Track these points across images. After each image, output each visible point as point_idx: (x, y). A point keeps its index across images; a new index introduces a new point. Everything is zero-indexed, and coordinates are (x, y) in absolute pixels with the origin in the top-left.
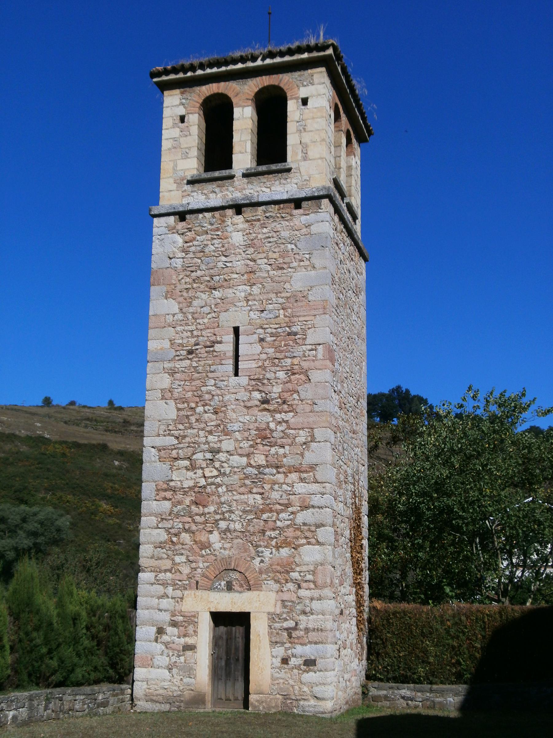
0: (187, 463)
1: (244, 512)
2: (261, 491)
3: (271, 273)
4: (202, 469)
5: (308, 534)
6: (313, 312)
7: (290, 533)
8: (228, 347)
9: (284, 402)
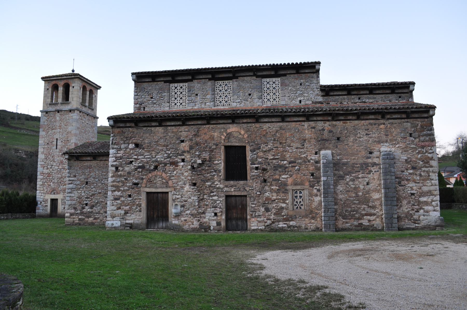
8: (55, 143)
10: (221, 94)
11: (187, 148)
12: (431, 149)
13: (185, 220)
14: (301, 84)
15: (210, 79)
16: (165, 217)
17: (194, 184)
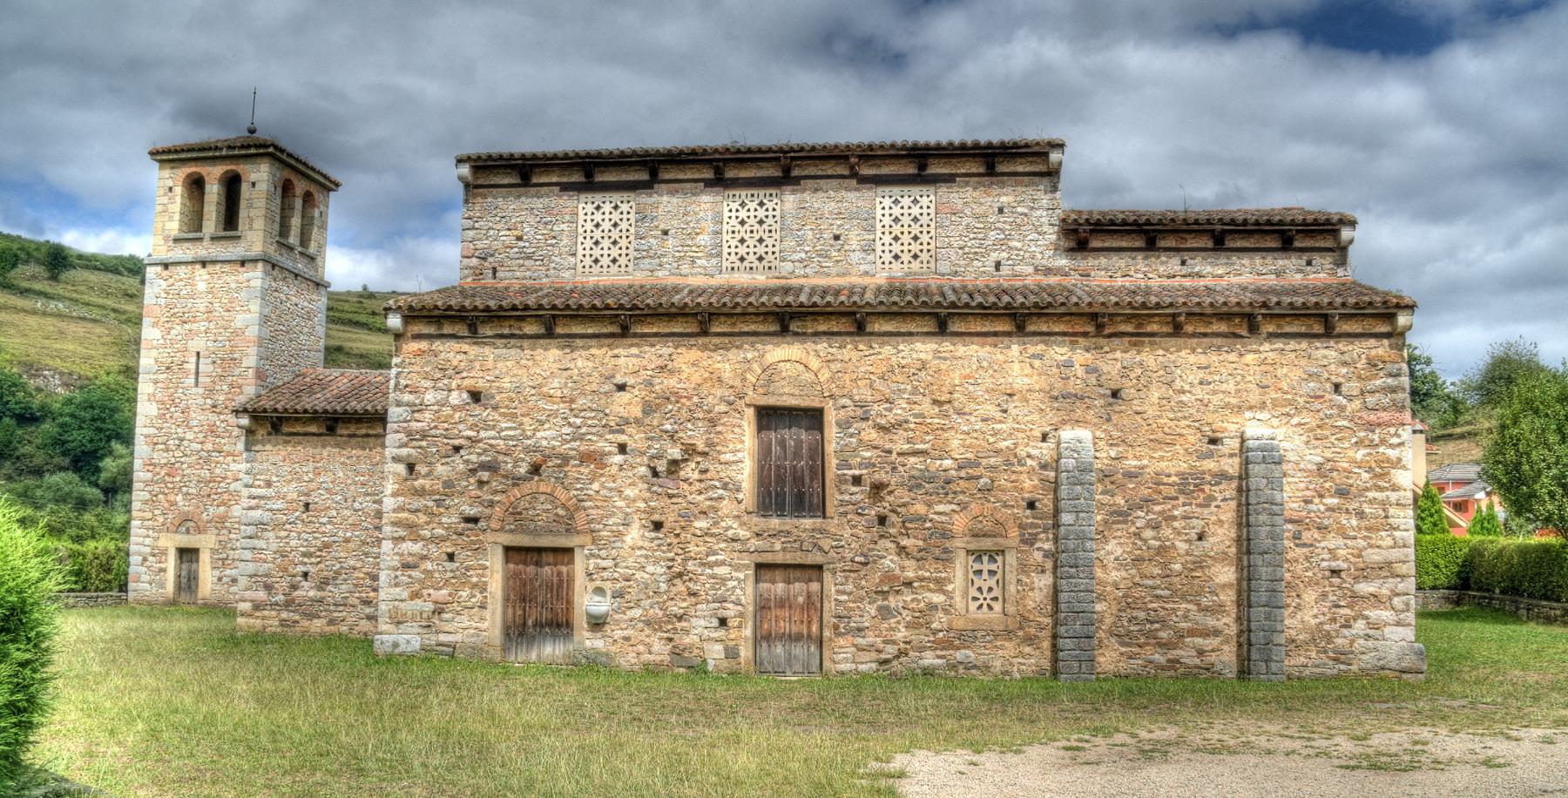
7: (226, 496)
8: (192, 367)
10: (742, 234)
11: (636, 411)
12: (1397, 435)
13: (627, 639)
14: (1001, 211)
15: (709, 184)
16: (560, 625)
17: (658, 526)
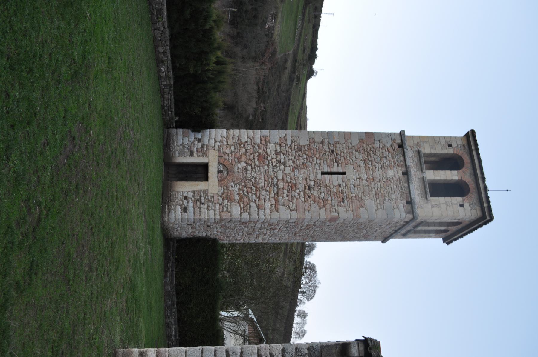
0: (279, 150)
1: (256, 178)
2: (266, 186)
3: (374, 190)
4: (276, 158)
5: (245, 208)
6: (354, 210)
7: (246, 200)
8: (335, 169)
9: (309, 197)
